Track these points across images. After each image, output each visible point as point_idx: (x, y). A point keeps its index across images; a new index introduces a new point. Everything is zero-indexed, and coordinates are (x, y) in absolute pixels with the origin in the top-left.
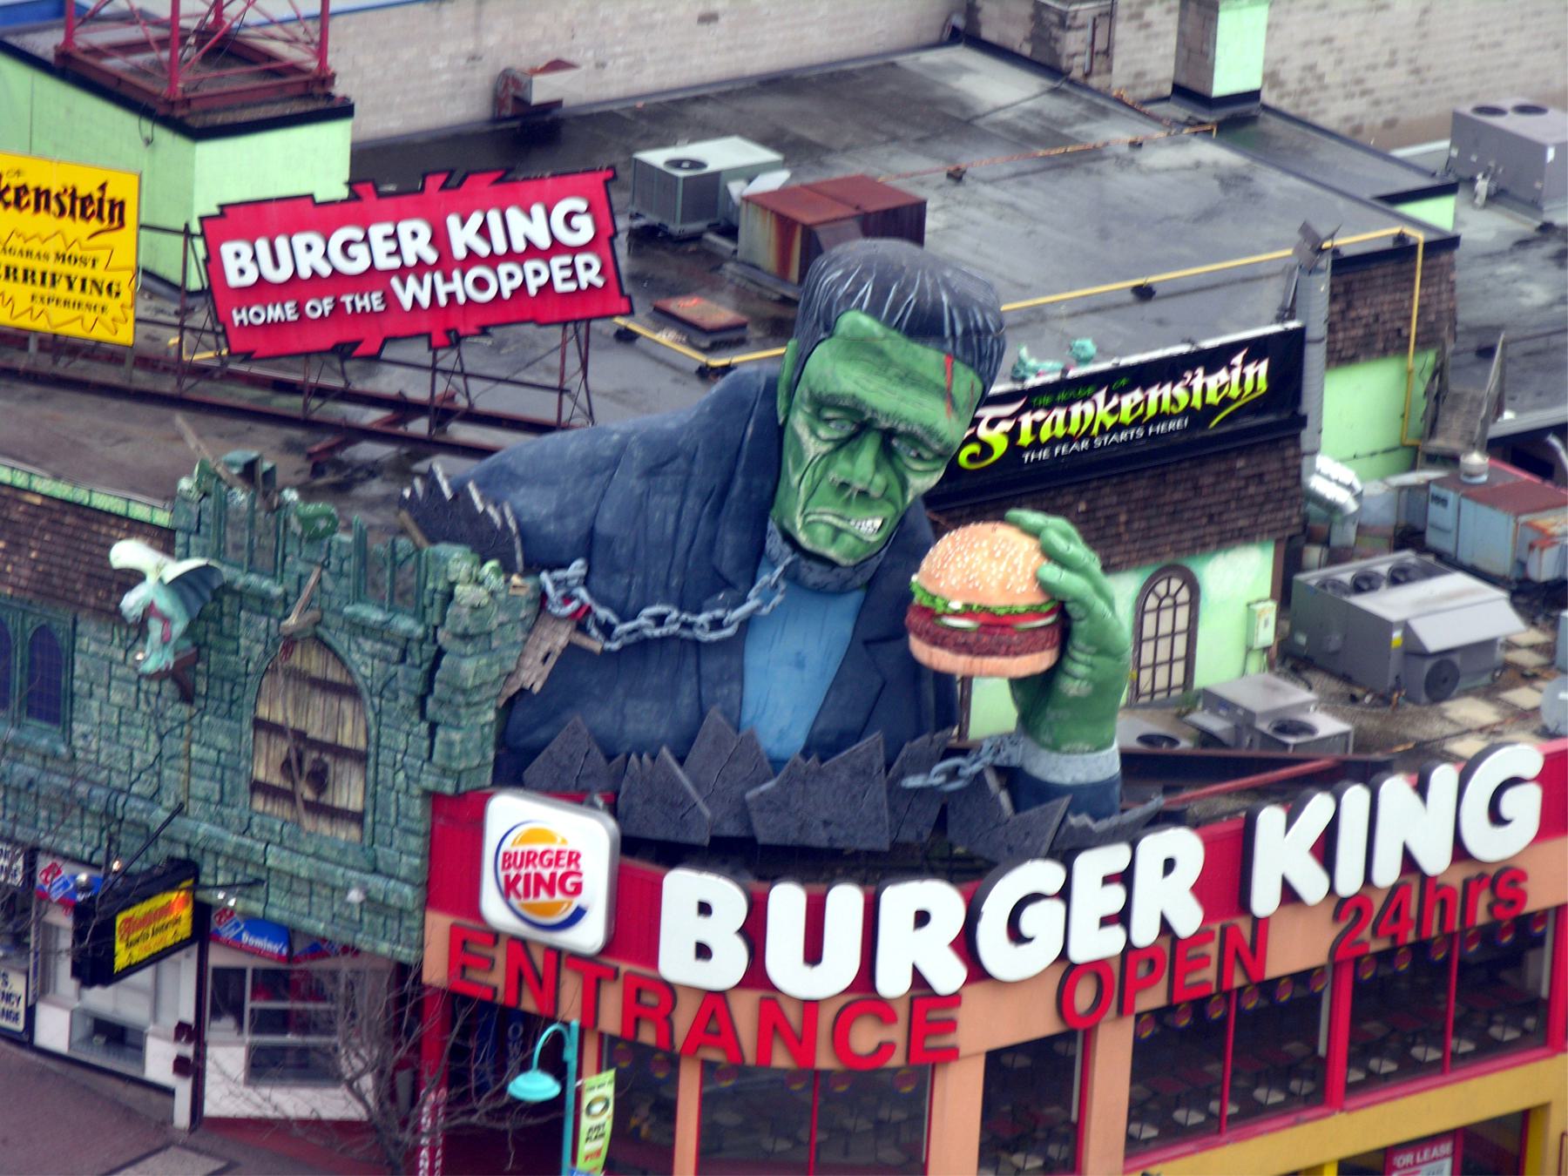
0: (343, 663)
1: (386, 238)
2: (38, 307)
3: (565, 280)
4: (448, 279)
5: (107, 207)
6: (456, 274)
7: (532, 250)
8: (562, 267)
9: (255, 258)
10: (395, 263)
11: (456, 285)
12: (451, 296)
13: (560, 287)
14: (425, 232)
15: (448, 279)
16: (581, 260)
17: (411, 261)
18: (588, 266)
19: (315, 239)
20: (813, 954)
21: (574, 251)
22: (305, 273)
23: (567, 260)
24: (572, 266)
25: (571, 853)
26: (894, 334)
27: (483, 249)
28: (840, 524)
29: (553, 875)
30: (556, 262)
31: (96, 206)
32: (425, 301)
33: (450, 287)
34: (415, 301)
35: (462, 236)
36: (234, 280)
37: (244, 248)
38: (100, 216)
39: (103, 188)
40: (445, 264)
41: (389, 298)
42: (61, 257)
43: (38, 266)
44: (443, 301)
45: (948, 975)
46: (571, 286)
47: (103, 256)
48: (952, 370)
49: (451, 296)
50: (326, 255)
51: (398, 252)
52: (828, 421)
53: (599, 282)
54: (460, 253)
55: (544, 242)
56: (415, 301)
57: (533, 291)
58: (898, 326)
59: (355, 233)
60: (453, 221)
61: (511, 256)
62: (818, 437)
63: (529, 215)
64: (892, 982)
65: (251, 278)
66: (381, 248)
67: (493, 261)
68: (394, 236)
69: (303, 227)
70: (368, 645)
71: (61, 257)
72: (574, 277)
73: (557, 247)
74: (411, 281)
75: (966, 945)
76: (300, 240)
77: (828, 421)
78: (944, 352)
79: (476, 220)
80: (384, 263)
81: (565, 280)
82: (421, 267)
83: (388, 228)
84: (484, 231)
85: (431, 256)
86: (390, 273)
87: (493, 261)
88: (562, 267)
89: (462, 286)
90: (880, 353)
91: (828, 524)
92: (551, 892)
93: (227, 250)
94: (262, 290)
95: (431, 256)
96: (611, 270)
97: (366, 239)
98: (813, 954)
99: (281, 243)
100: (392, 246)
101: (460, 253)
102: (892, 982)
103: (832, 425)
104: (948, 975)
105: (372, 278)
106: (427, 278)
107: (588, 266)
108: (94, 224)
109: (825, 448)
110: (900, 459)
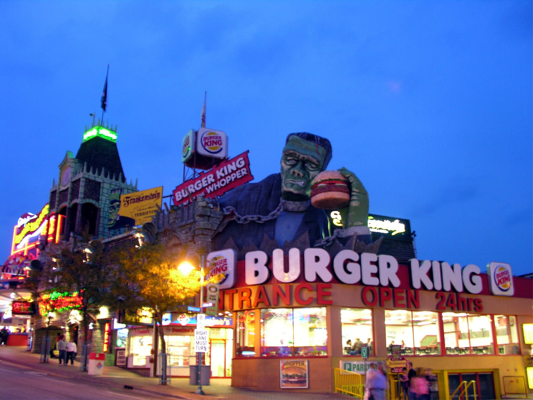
0: (178, 238)
1: (205, 180)
2: (145, 219)
3: (239, 175)
4: (217, 184)
5: (157, 194)
6: (218, 182)
7: (233, 172)
8: (239, 173)
9: (181, 194)
10: (207, 184)
11: (218, 185)
12: (217, 187)
13: (239, 177)
14: (212, 176)
15: (217, 184)
16: (242, 170)
17: (209, 183)
18: (244, 171)
19: (192, 186)
20: (286, 269)
21: (240, 169)
23: (239, 171)
24: (241, 172)
25: (224, 260)
26: (303, 139)
27: (223, 175)
28: (294, 183)
29: (220, 266)
30: (237, 172)
31: (155, 196)
32: (212, 190)
33: (217, 186)
34: (211, 191)
35: (219, 174)
36: (178, 199)
37: (179, 193)
38: (155, 197)
39: (156, 192)
40: (216, 180)
41: (206, 192)
42: (149, 208)
43: (145, 211)
44: (216, 189)
45: (327, 277)
46: (241, 176)
48: (318, 147)
49: (217, 187)
50: (194, 188)
51: (207, 182)
52: (289, 160)
53: (246, 173)
54: (219, 177)
55: (235, 169)
56: (211, 191)
57: (233, 180)
58: (303, 138)
59: (199, 181)
60: (217, 172)
61: (229, 174)
62: (286, 164)
63: (232, 165)
64: (310, 277)
67: (225, 177)
68: (207, 179)
69: (190, 184)
70: (184, 232)
71: (149, 208)
72: (241, 174)
73: (238, 169)
74: (210, 187)
75: (331, 268)
76: (189, 187)
77: (289, 160)
78: (315, 143)
79: (222, 170)
80: (205, 185)
81: (239, 175)
82: (212, 183)
83: (205, 178)
84: (223, 172)
85: (213, 180)
86: (205, 187)
87: (225, 177)
88: (239, 173)
89: (220, 184)
90: (300, 143)
91: (290, 183)
92: (220, 272)
93: (176, 194)
94: (183, 199)
95: (213, 180)
96: (249, 172)
97: (201, 182)
98: (286, 269)
100: (206, 181)
101: (219, 177)
102: (310, 277)
103: (290, 161)
104: (327, 277)
105: (203, 189)
106: (213, 185)
107: (244, 171)
108: (155, 199)
109: (289, 167)
110: (307, 168)
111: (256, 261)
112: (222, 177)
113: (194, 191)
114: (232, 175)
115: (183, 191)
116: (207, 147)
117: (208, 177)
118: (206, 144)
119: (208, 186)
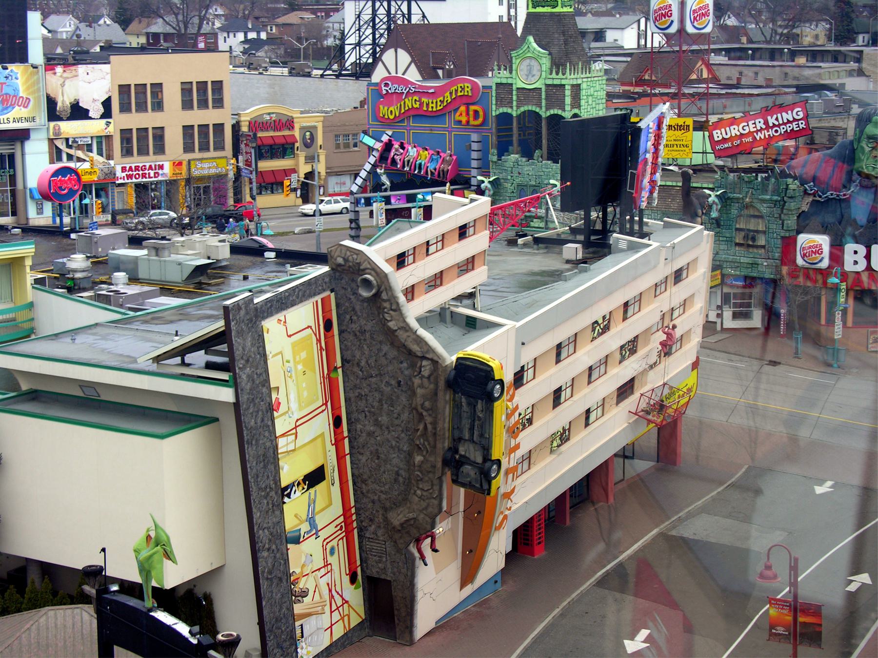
10: (755, 129)
12: (769, 135)
13: (795, 129)
14: (762, 121)
19: (735, 127)
22: (733, 135)
27: (777, 123)
37: (719, 131)
47: (684, 138)
49: (769, 135)
51: (756, 127)
55: (791, 119)
65: (720, 138)
66: (751, 126)
73: (795, 120)
76: (732, 128)
83: (753, 122)
84: (777, 119)
99: (728, 129)
111: (856, 252)
112: (774, 125)
113: (738, 134)
114: (788, 125)
115: (723, 130)
116: (696, 24)
117: (757, 121)
118: (695, 19)
119: (757, 131)
